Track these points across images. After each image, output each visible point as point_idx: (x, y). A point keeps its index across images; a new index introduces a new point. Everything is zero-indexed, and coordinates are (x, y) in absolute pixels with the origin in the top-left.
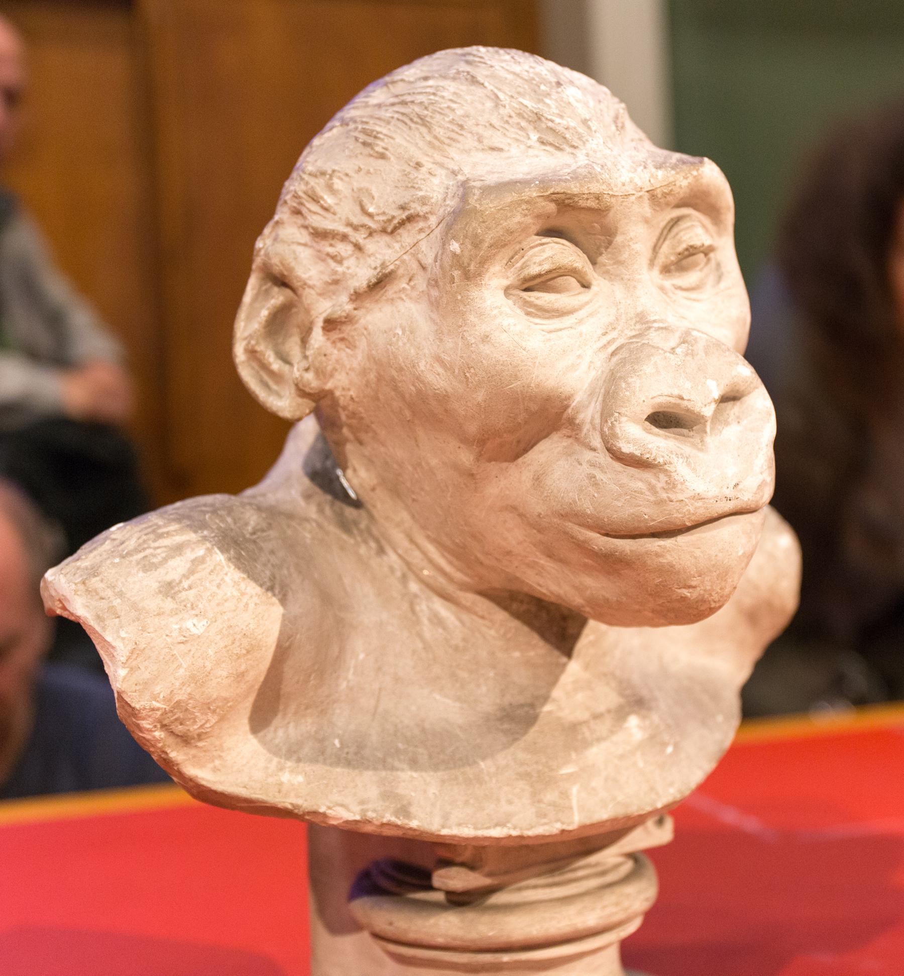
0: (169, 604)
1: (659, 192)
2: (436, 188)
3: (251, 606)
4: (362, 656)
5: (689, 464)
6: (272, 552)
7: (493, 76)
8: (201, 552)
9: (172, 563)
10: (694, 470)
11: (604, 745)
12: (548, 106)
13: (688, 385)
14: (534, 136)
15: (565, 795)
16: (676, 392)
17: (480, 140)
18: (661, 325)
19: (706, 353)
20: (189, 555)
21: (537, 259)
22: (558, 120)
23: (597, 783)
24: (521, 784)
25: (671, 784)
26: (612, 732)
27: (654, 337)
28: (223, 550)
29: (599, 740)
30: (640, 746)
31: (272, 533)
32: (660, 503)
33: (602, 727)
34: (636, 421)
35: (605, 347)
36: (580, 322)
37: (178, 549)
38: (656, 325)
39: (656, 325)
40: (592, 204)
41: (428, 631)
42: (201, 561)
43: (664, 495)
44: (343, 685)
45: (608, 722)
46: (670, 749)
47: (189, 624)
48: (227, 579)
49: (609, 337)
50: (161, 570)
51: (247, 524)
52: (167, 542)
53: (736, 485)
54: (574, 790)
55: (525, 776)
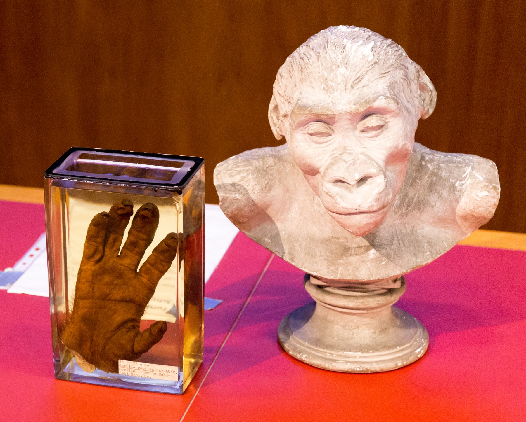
0: (233, 189)
1: (352, 113)
2: (296, 96)
3: (256, 193)
4: (297, 209)
5: (341, 198)
6: (272, 175)
7: (325, 57)
8: (245, 174)
9: (237, 176)
10: (343, 200)
11: (357, 257)
12: (330, 76)
13: (347, 174)
14: (323, 87)
15: (337, 269)
16: (343, 176)
17: (311, 83)
18: (350, 152)
19: (360, 164)
20: (242, 175)
21: (312, 128)
22: (330, 83)
23: (350, 268)
24: (325, 262)
25: (379, 274)
26: (362, 253)
27: (345, 157)
28: (253, 174)
29: (356, 255)
30: (372, 260)
31: (275, 167)
32: (334, 206)
33: (360, 251)
34: (328, 182)
35: (331, 155)
36: (327, 146)
37: (239, 172)
38: (348, 152)
39: (348, 152)
40: (326, 117)
41: (316, 207)
42: (245, 177)
43: (335, 205)
44: (290, 216)
45: (363, 250)
46: (384, 263)
47: (237, 195)
48: (250, 184)
49: (334, 152)
50: (233, 178)
51: (267, 164)
52: (238, 169)
53: (359, 206)
54: (341, 268)
55: (327, 260)
